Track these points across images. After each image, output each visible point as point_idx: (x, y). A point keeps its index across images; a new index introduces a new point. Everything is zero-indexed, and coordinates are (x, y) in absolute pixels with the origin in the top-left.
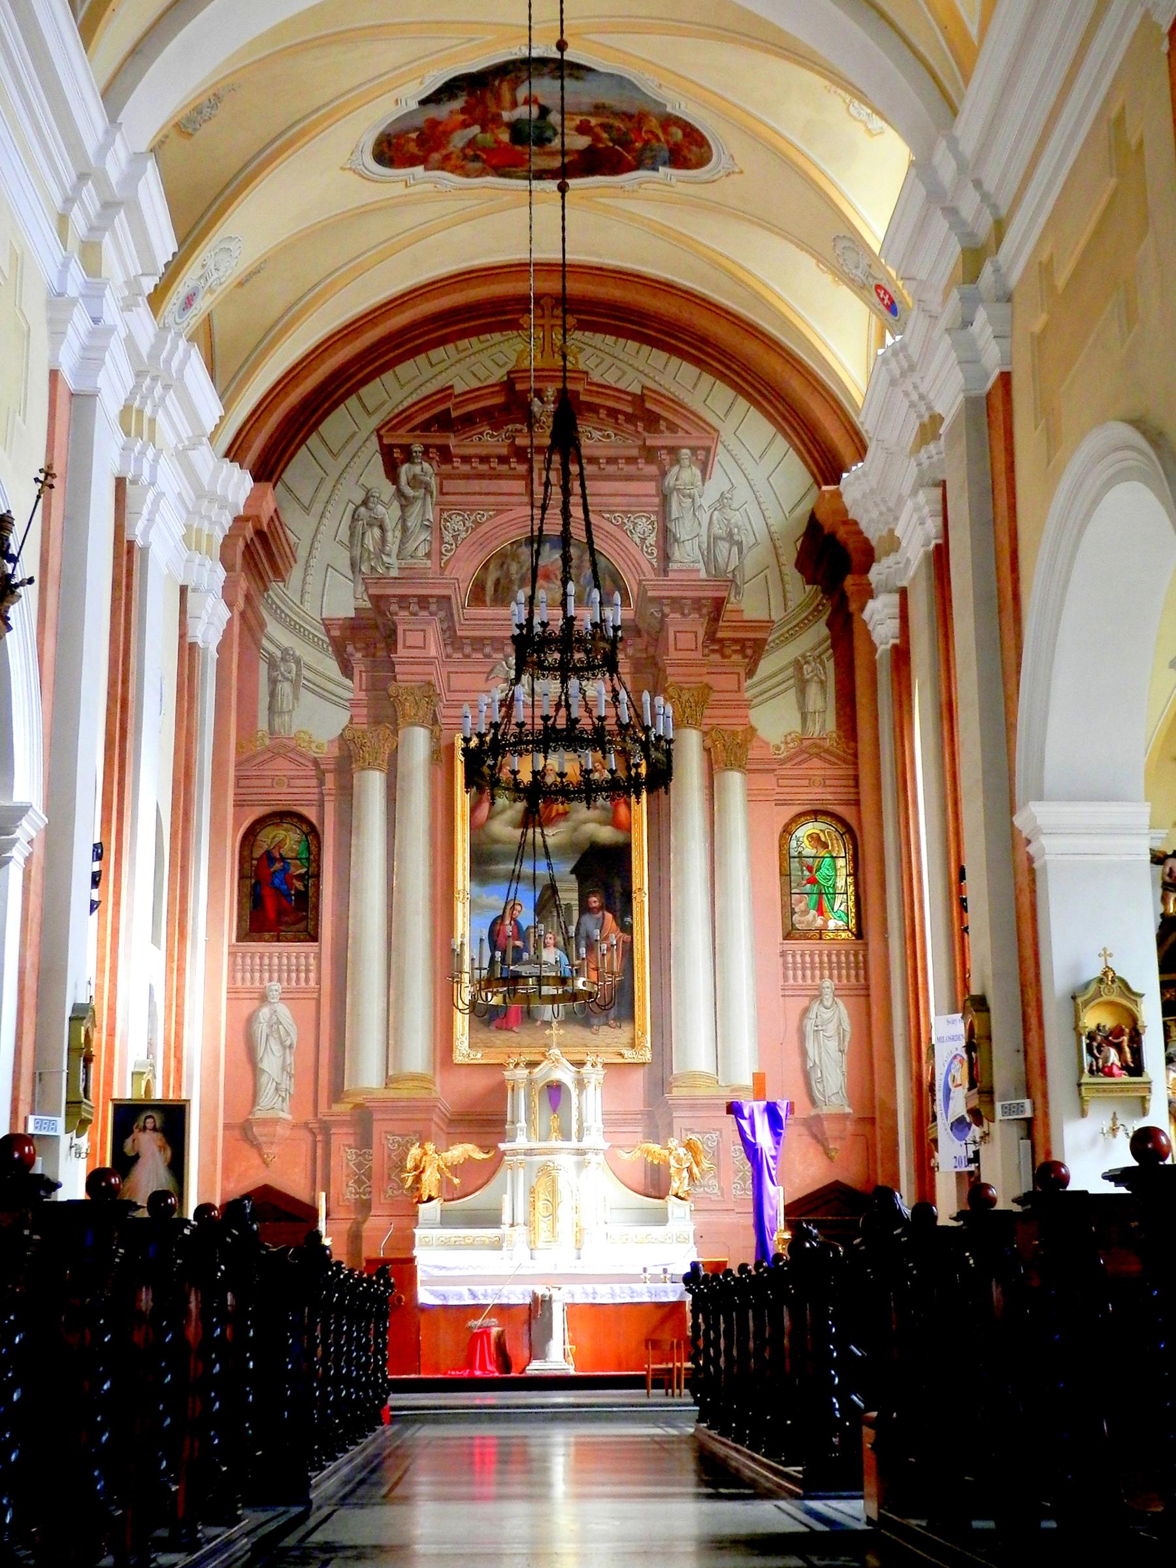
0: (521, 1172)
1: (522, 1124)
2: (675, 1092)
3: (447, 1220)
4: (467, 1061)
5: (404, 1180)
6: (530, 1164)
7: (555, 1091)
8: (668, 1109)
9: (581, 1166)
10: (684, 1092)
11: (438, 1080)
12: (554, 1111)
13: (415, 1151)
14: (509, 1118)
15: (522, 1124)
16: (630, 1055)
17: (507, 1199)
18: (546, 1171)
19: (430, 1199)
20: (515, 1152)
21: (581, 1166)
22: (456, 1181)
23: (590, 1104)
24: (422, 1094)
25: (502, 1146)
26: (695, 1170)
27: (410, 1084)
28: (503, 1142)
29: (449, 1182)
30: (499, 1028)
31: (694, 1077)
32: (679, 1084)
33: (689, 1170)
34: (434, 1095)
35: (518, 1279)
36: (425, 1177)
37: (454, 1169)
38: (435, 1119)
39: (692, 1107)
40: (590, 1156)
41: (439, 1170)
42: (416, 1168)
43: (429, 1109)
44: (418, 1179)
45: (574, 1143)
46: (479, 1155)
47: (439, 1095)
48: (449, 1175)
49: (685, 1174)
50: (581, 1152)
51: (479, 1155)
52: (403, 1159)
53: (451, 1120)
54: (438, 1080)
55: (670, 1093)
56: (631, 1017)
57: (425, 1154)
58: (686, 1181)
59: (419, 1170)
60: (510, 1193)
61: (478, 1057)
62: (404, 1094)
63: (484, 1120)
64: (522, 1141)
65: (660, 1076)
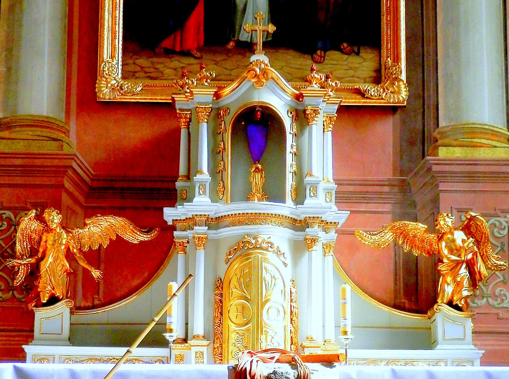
0: (201, 254)
1: (204, 175)
2: (443, 153)
3: (77, 337)
4: (119, 98)
5: (12, 272)
6: (217, 242)
7: (257, 130)
8: (433, 178)
9: (302, 247)
10: (457, 153)
11: (73, 127)
12: (257, 157)
13: (28, 223)
14: (182, 170)
15: (204, 175)
16: (377, 96)
17: (175, 308)
18: (243, 249)
19: (53, 300)
20: (191, 222)
21: (302, 247)
22: (96, 274)
23: (316, 151)
24: (50, 147)
25: (170, 214)
26: (480, 266)
27: (28, 133)
28: (172, 204)
29: (86, 273)
30: (169, 53)
31: (471, 133)
32: (446, 141)
33: (470, 265)
34: (66, 150)
35: (182, 214)
36: (45, 266)
37: (93, 257)
38: (67, 184)
39: (471, 177)
40: (315, 231)
41: (69, 256)
42: (33, 252)
43: (61, 171)
44: (34, 272)
45: (287, 208)
46: (135, 237)
47: (74, 150)
48: (83, 264)
49: (463, 271)
50: (299, 225)
51: (135, 237)
52: (11, 241)
53: (92, 188)
54: (73, 127)
55: (436, 155)
56: (375, 43)
57: (48, 230)
58: (466, 283)
59: (36, 252)
60: (180, 299)
61: (137, 92)
62: (19, 147)
63: (143, 183)
64: (201, 204)
65: (419, 128)
